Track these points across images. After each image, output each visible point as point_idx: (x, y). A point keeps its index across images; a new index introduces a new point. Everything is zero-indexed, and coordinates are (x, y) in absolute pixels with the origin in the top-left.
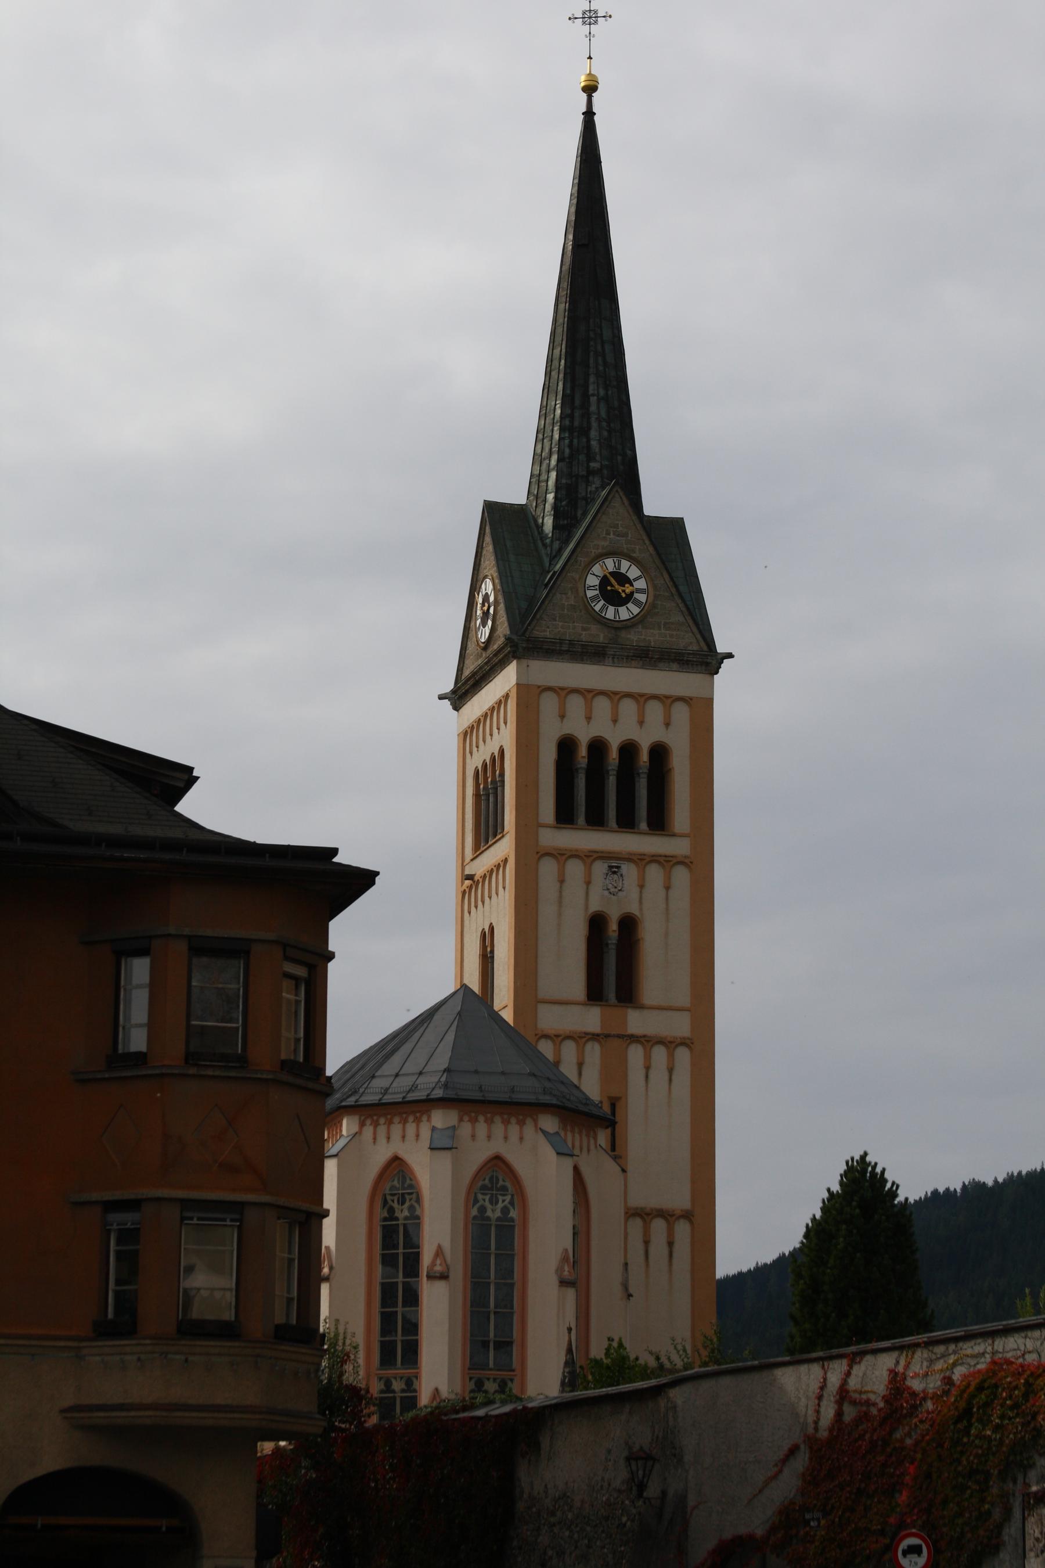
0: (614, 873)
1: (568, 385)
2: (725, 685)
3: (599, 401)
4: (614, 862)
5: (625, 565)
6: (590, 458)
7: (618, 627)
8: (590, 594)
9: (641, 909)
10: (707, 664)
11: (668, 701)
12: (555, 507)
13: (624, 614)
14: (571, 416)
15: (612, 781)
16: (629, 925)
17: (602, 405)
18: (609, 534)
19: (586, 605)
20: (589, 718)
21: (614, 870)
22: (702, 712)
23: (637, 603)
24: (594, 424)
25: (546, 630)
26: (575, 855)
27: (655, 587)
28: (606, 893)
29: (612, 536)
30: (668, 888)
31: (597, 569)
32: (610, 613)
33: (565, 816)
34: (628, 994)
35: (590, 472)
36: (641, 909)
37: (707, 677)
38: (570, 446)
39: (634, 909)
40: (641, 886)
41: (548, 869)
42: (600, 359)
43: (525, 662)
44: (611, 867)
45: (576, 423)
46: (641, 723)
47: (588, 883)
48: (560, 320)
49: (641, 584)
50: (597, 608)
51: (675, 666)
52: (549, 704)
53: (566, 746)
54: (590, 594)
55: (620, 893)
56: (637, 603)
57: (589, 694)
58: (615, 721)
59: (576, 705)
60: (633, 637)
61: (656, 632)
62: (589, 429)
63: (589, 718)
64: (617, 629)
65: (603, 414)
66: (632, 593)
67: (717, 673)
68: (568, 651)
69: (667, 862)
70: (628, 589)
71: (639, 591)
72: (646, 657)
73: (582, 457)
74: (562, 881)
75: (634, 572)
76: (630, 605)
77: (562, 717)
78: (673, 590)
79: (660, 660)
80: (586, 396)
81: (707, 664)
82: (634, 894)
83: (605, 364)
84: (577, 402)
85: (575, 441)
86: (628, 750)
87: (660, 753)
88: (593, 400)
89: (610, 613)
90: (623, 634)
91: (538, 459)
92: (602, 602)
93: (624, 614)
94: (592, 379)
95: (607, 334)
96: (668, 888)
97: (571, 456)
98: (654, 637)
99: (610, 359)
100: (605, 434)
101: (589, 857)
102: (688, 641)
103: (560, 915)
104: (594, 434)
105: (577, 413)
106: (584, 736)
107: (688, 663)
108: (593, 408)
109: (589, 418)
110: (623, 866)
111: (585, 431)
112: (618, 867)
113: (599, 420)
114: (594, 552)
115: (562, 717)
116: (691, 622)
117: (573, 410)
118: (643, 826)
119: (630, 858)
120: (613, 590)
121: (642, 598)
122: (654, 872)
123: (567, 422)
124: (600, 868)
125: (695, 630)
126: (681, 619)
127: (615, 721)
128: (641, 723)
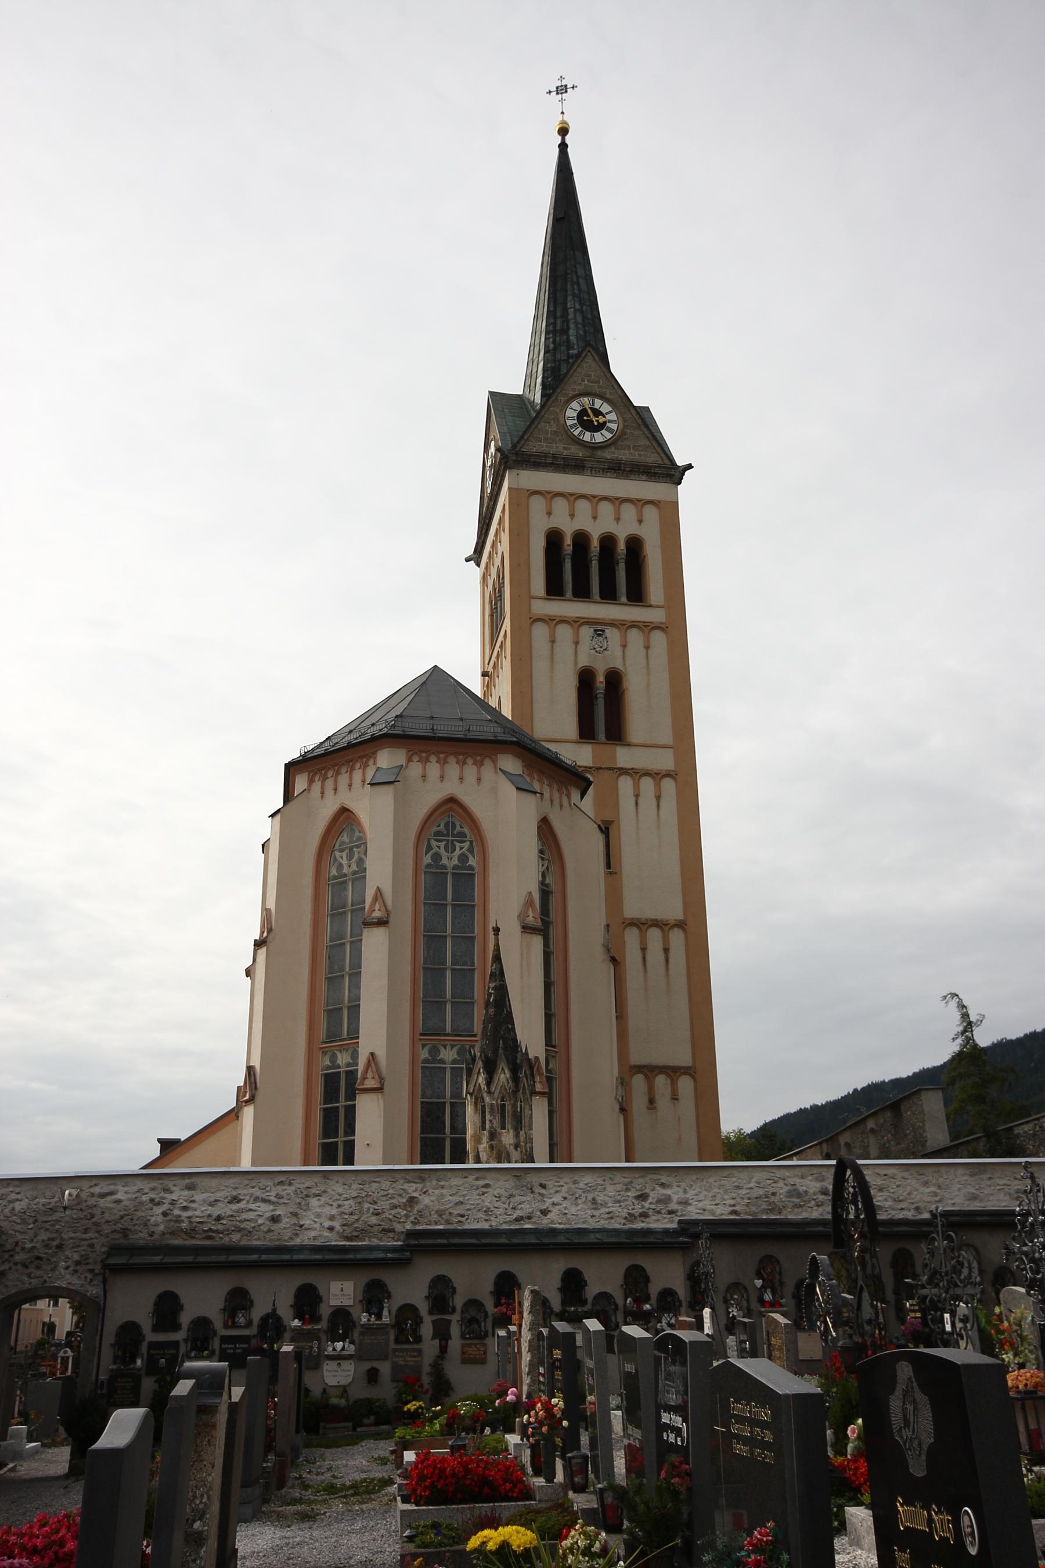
0: (600, 635)
1: (552, 305)
2: (687, 492)
3: (575, 311)
4: (599, 628)
5: (598, 403)
6: (569, 346)
7: (595, 447)
8: (569, 423)
9: (624, 665)
10: (671, 476)
11: (641, 503)
12: (543, 384)
13: (598, 437)
14: (555, 324)
15: (595, 565)
16: (615, 679)
17: (578, 314)
18: (583, 380)
19: (566, 431)
20: (572, 516)
21: (599, 633)
22: (669, 513)
23: (610, 430)
24: (572, 326)
25: (533, 447)
26: (563, 621)
27: (625, 421)
28: (593, 651)
30: (647, 648)
31: (575, 405)
32: (587, 437)
33: (554, 589)
34: (616, 733)
35: (569, 357)
37: (673, 486)
38: (554, 342)
39: (618, 664)
40: (624, 646)
41: (540, 632)
42: (575, 287)
43: (515, 472)
45: (558, 327)
46: (618, 519)
47: (577, 643)
48: (545, 270)
49: (613, 416)
50: (576, 433)
51: (644, 477)
52: (537, 505)
53: (554, 539)
54: (569, 423)
56: (610, 430)
57: (573, 498)
58: (595, 518)
59: (560, 506)
60: (607, 454)
61: (627, 452)
62: (568, 328)
63: (572, 516)
64: (593, 448)
65: (579, 319)
66: (605, 423)
67: (680, 483)
68: (552, 464)
69: (646, 628)
70: (601, 419)
71: (610, 421)
72: (618, 469)
73: (563, 348)
74: (553, 642)
75: (605, 408)
76: (603, 432)
77: (549, 514)
78: (639, 421)
79: (631, 472)
80: (565, 310)
81: (671, 476)
82: (618, 652)
83: (580, 290)
84: (559, 314)
85: (558, 339)
86: (608, 542)
87: (635, 545)
88: (571, 311)
89: (587, 437)
90: (599, 453)
91: (531, 362)
92: (580, 429)
93: (598, 437)
94: (569, 298)
95: (581, 272)
96: (647, 648)
97: (555, 349)
98: (624, 455)
99: (583, 287)
100: (581, 332)
101: (577, 623)
102: (652, 459)
103: (552, 669)
104: (571, 332)
105: (559, 322)
106: (568, 529)
107: (655, 474)
108: (571, 316)
109: (568, 323)
111: (565, 331)
112: (603, 631)
113: (576, 323)
114: (571, 393)
115: (549, 514)
116: (655, 444)
117: (555, 318)
118: (624, 599)
119: (612, 624)
120: (586, 421)
121: (614, 426)
122: (634, 635)
123: (551, 328)
124: (586, 632)
125: (660, 451)
126: (647, 443)
127: (595, 518)
128: (618, 519)
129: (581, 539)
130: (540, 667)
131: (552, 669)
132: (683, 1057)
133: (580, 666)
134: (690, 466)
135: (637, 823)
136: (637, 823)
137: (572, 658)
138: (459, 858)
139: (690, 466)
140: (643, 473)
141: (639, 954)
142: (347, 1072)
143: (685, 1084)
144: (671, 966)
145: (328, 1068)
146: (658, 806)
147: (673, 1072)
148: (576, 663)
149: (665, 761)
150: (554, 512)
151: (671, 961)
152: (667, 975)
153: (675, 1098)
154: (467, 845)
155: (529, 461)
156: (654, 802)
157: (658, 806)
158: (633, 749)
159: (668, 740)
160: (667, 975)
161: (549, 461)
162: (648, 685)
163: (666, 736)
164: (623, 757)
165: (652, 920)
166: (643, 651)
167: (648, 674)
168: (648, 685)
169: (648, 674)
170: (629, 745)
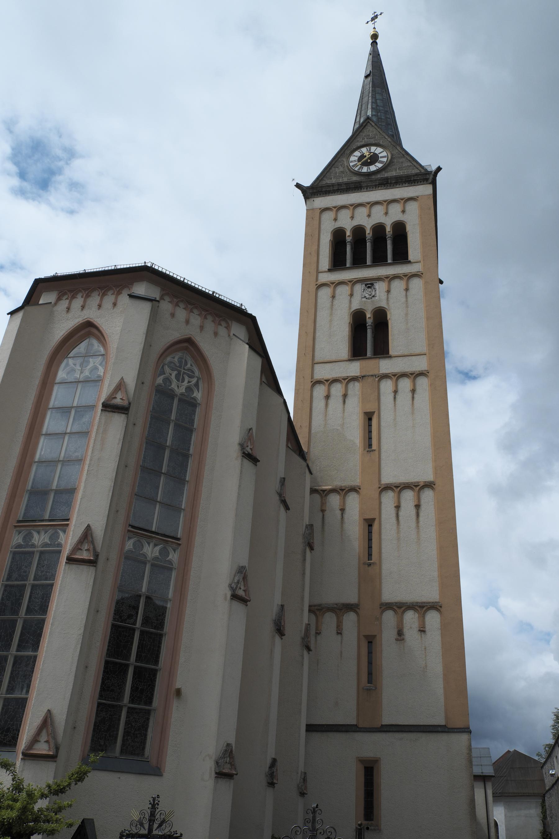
0: (369, 287)
4: (369, 283)
5: (373, 149)
9: (388, 304)
23: (381, 162)
28: (364, 299)
29: (366, 139)
31: (357, 154)
36: (388, 304)
39: (383, 304)
44: (366, 285)
55: (373, 299)
56: (381, 162)
86: (379, 229)
110: (375, 284)
112: (372, 284)
119: (379, 279)
129: (359, 231)
130: (323, 315)
131: (331, 314)
132: (431, 594)
133: (353, 309)
134: (439, 169)
135: (395, 411)
136: (395, 411)
137: (347, 305)
138: (186, 389)
139: (439, 169)
140: (405, 182)
141: (393, 511)
142: (42, 553)
143: (433, 619)
144: (421, 519)
145: (19, 546)
146: (413, 398)
147: (422, 608)
148: (350, 308)
149: (420, 364)
150: (338, 218)
151: (421, 514)
152: (418, 526)
153: (422, 631)
154: (194, 381)
155: (321, 191)
156: (410, 395)
157: (413, 398)
158: (394, 359)
159: (425, 350)
160: (418, 526)
161: (336, 188)
162: (407, 315)
163: (421, 345)
164: (385, 366)
165: (404, 483)
166: (404, 293)
167: (407, 307)
168: (407, 315)
169: (407, 307)
170: (390, 357)
